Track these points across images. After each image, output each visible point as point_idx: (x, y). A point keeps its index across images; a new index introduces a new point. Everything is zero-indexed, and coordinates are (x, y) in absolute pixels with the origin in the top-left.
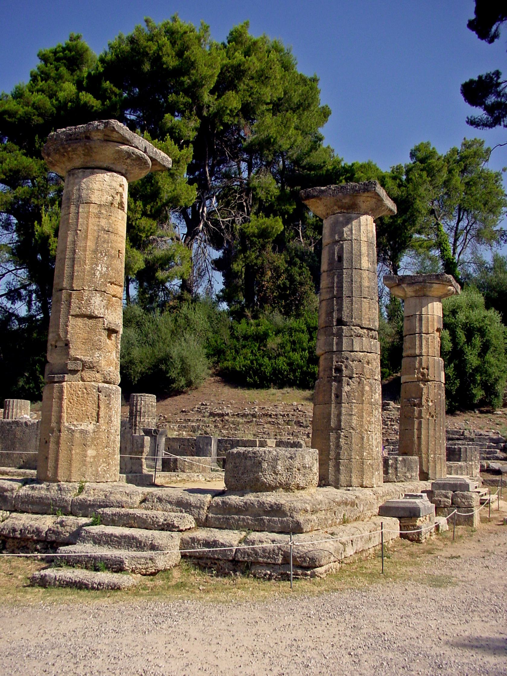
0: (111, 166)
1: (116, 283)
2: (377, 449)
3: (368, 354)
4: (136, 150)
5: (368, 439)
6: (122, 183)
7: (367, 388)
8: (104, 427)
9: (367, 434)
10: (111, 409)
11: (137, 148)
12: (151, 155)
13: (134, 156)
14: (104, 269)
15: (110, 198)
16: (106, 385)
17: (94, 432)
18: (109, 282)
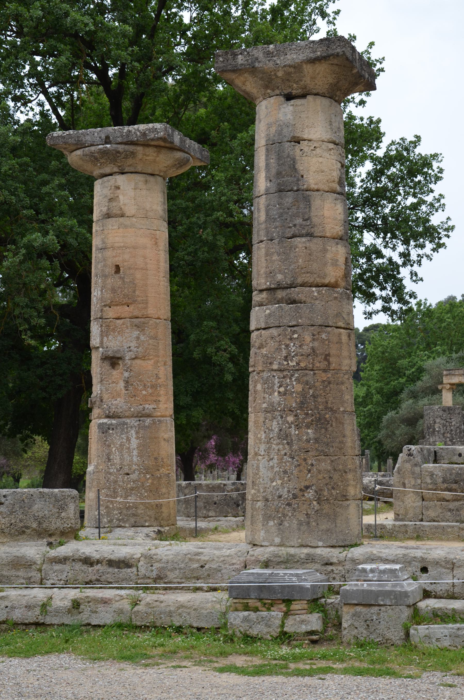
0: (102, 171)
1: (114, 303)
2: (274, 484)
3: (263, 332)
4: (93, 148)
5: (258, 467)
6: (117, 184)
7: (259, 387)
8: (101, 467)
9: (258, 460)
10: (109, 446)
11: (92, 145)
12: (119, 140)
13: (96, 155)
14: (99, 293)
15: (105, 209)
16: (105, 421)
17: (94, 473)
18: (105, 306)
